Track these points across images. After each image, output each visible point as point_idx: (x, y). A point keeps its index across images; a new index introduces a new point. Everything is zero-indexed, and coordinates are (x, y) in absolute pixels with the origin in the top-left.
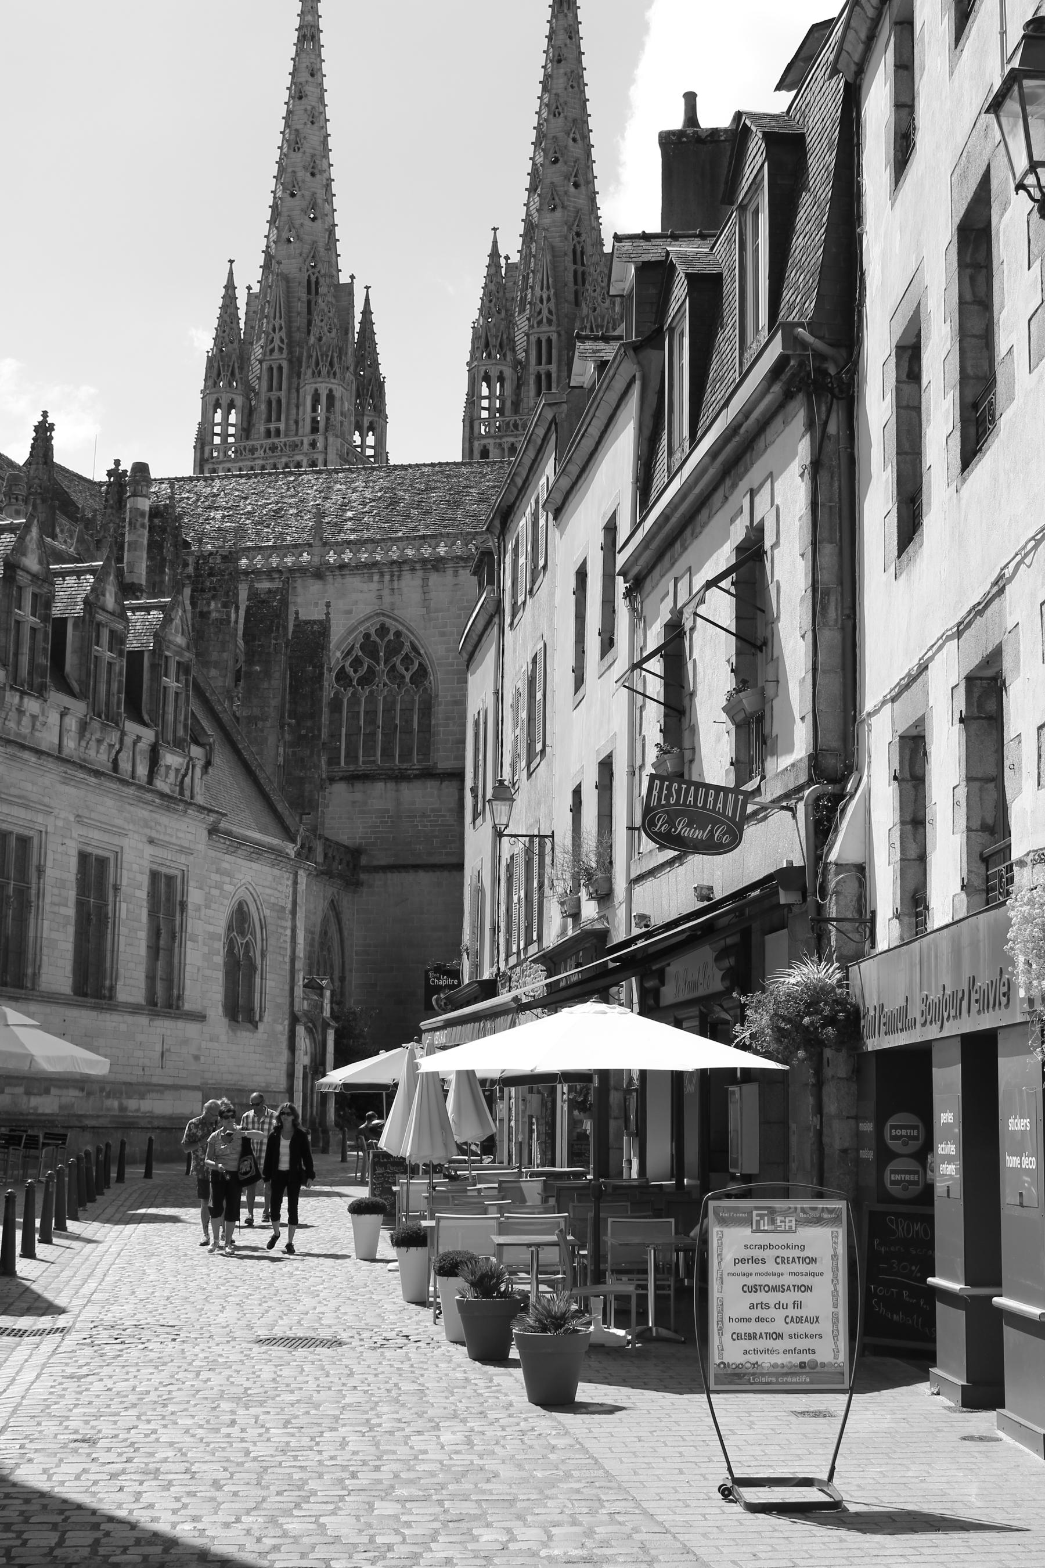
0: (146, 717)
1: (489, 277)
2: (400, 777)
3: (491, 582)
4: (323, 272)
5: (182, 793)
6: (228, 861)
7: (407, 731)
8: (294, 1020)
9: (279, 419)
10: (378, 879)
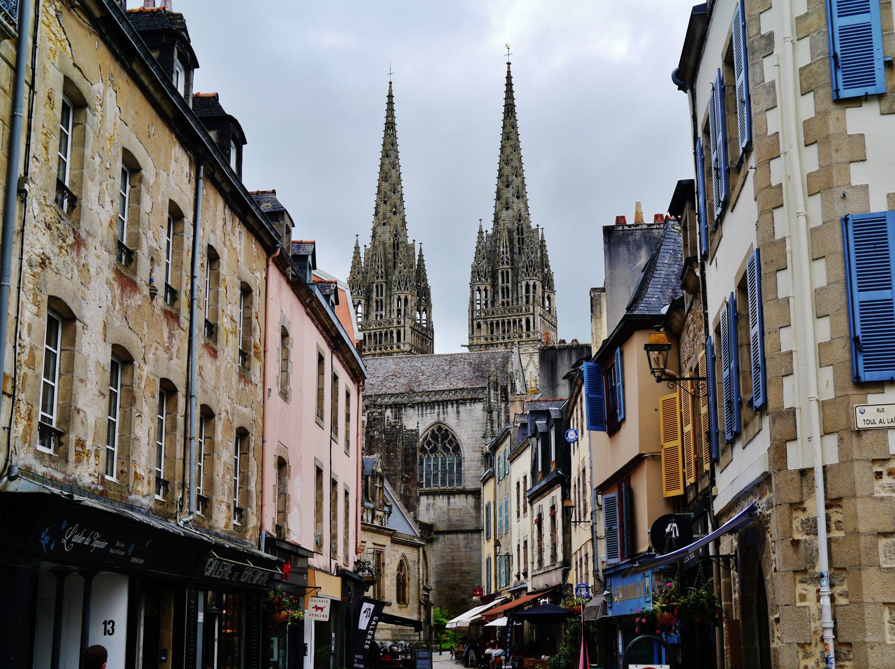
0: (370, 499)
1: (479, 242)
2: (449, 494)
3: (491, 466)
4: (400, 240)
5: (382, 525)
6: (396, 547)
7: (451, 472)
8: (420, 603)
9: (382, 310)
10: (441, 537)
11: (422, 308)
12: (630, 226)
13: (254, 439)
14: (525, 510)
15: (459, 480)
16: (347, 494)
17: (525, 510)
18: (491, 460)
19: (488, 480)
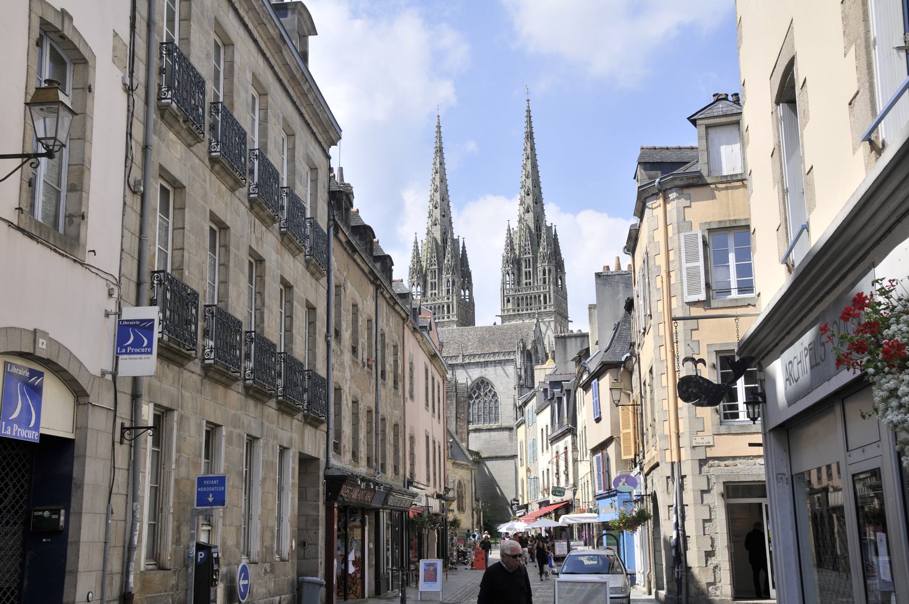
3: (523, 415)
6: (457, 470)
8: (473, 510)
9: (435, 289)
11: (466, 288)
12: (612, 272)
13: (401, 429)
14: (547, 448)
15: (496, 419)
16: (439, 447)
17: (547, 448)
18: (523, 411)
19: (520, 425)
